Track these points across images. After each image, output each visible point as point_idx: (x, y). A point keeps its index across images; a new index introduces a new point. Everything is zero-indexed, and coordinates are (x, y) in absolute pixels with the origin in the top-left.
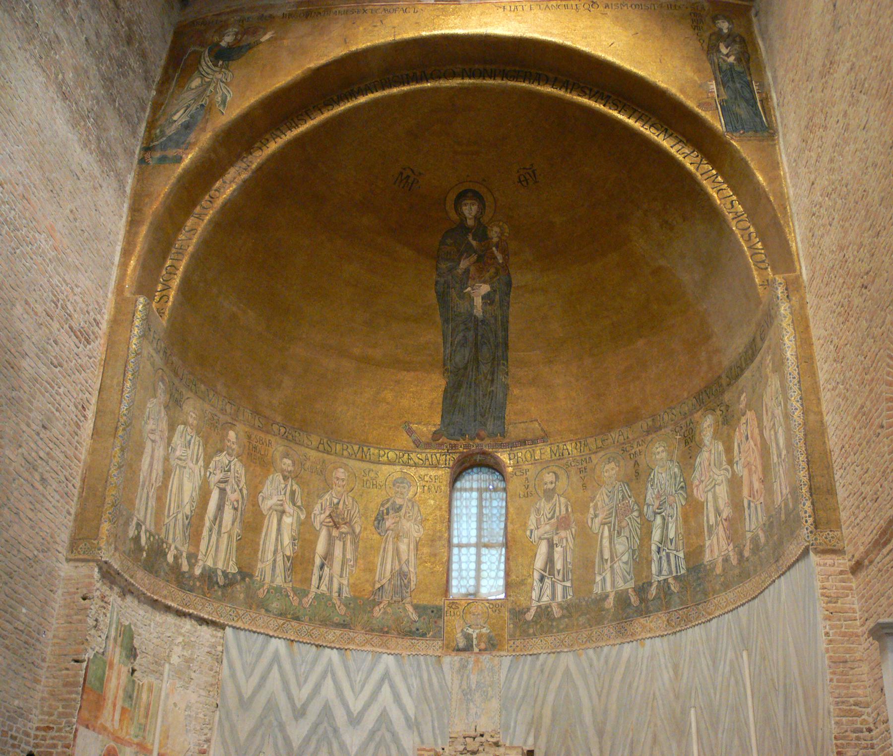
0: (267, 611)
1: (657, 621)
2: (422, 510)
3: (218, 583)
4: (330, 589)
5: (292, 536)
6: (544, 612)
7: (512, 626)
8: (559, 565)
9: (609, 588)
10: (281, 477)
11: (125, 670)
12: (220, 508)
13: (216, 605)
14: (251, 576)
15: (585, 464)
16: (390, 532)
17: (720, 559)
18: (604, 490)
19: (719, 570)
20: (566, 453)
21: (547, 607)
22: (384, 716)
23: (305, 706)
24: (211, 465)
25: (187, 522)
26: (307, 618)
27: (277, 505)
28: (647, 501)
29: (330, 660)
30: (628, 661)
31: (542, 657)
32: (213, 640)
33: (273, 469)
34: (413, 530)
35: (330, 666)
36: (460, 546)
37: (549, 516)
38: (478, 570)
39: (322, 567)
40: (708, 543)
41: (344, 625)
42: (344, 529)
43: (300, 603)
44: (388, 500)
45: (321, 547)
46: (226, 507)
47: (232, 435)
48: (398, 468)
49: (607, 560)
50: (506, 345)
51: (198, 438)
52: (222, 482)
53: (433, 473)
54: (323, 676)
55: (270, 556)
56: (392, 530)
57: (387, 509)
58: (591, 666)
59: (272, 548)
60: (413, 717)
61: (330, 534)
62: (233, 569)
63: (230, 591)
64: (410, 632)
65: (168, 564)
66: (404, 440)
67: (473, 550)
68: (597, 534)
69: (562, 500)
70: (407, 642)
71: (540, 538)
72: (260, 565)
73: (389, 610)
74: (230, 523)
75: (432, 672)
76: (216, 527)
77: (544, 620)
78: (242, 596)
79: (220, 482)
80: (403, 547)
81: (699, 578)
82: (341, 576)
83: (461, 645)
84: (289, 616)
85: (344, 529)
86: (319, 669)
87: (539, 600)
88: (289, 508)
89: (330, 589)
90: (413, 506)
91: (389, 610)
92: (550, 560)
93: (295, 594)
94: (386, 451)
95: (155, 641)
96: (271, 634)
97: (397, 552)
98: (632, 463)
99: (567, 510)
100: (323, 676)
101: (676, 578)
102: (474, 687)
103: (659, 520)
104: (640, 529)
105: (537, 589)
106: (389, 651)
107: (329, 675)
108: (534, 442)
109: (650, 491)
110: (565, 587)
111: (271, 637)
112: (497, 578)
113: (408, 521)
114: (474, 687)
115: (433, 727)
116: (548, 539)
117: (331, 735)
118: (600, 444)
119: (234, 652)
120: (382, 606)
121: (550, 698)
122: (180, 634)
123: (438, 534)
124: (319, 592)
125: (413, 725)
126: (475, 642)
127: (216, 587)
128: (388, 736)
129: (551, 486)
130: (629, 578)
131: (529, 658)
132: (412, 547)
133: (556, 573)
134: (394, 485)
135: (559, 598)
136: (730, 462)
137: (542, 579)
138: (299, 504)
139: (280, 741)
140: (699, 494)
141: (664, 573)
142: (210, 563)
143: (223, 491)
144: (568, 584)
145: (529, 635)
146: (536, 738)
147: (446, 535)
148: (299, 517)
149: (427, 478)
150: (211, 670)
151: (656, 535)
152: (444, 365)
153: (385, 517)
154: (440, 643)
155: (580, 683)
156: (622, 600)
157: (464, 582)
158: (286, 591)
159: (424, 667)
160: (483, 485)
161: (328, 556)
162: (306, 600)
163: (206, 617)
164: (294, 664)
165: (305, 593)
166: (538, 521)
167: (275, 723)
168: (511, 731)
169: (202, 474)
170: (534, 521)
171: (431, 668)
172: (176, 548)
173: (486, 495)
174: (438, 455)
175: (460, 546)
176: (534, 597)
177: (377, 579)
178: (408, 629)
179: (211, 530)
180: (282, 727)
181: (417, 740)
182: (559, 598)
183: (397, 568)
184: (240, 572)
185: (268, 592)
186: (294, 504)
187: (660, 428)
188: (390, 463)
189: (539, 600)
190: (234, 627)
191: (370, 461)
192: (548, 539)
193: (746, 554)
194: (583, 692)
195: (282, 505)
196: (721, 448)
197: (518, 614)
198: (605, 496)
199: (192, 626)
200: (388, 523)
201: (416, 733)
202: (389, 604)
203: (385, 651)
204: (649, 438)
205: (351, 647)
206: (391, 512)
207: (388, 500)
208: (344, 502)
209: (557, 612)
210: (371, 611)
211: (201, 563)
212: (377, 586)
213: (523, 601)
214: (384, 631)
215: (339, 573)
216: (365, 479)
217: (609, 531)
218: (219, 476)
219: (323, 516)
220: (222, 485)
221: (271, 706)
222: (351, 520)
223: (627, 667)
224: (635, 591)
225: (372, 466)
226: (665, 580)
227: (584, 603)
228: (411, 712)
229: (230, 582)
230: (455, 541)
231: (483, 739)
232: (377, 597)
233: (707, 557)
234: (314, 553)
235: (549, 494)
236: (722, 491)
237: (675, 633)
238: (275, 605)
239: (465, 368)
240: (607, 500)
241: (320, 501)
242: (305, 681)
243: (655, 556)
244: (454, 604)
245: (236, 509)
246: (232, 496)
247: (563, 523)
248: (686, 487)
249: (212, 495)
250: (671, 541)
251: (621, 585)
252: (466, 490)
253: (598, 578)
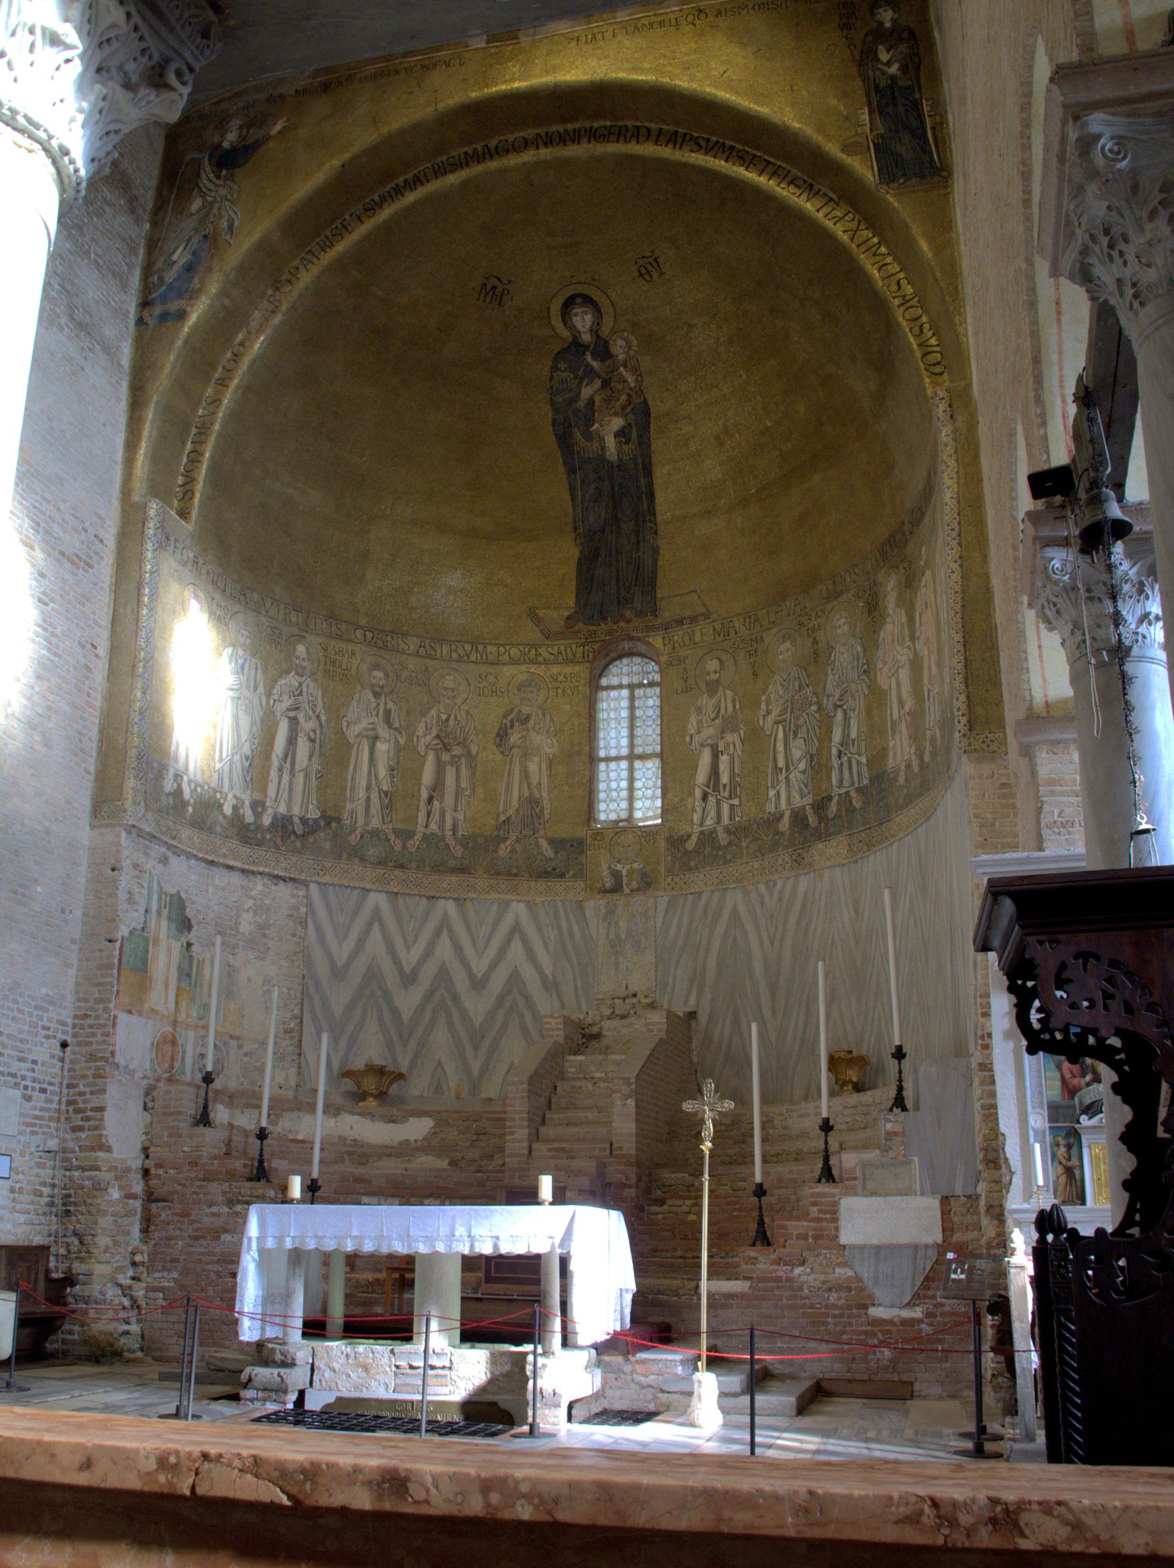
0: (362, 859)
1: (836, 847)
2: (555, 719)
3: (294, 832)
4: (442, 826)
5: (390, 766)
6: (708, 838)
7: (669, 858)
8: (725, 779)
9: (783, 805)
10: (371, 695)
11: (177, 946)
12: (292, 742)
13: (294, 859)
14: (338, 820)
15: (755, 646)
16: (515, 750)
17: (903, 766)
18: (777, 678)
19: (901, 780)
20: (732, 632)
21: (711, 832)
22: (515, 977)
23: (415, 971)
24: (275, 691)
25: (247, 764)
26: (414, 865)
27: (368, 730)
28: (828, 691)
29: (446, 914)
30: (805, 898)
31: (705, 896)
32: (294, 901)
33: (359, 686)
34: (545, 744)
35: (445, 919)
36: (608, 759)
37: (712, 716)
38: (631, 789)
39: (430, 800)
40: (891, 744)
41: (462, 870)
42: (457, 751)
43: (404, 847)
44: (512, 710)
45: (428, 776)
46: (300, 740)
47: (301, 649)
48: (523, 668)
49: (781, 769)
50: (651, 496)
51: (254, 660)
52: (292, 710)
53: (567, 670)
54: (437, 934)
55: (362, 793)
56: (519, 747)
57: (512, 721)
58: (762, 904)
59: (364, 783)
60: (551, 978)
61: (438, 759)
62: (314, 813)
63: (311, 840)
64: (545, 872)
65: (225, 817)
66: (531, 633)
67: (624, 764)
68: (770, 736)
69: (729, 693)
70: (541, 885)
71: (702, 745)
72: (349, 806)
73: (518, 848)
74: (306, 759)
75: (573, 921)
76: (288, 765)
77: (708, 850)
78: (328, 845)
79: (289, 710)
80: (533, 768)
81: (882, 790)
82: (455, 810)
83: (608, 885)
84: (391, 864)
85: (457, 751)
86: (431, 925)
87: (701, 825)
88: (383, 732)
89: (442, 826)
90: (544, 714)
91: (518, 848)
92: (715, 772)
93: (397, 836)
94: (508, 648)
95: (216, 908)
96: (368, 886)
97: (525, 774)
98: (810, 640)
99: (734, 706)
100: (437, 934)
101: (858, 790)
102: (623, 936)
103: (840, 715)
104: (819, 727)
105: (699, 810)
106: (519, 898)
107: (445, 931)
108: (693, 619)
109: (830, 677)
110: (732, 806)
111: (369, 891)
112: (653, 798)
113: (538, 733)
114: (623, 936)
115: (576, 987)
116: (712, 746)
117: (450, 1003)
118: (773, 617)
119: (321, 912)
120: (508, 843)
121: (716, 944)
122: (251, 897)
123: (576, 748)
124: (428, 831)
125: (550, 985)
126: (625, 880)
127: (293, 838)
128: (520, 1001)
129: (714, 677)
130: (806, 791)
131: (690, 897)
132: (544, 766)
133: (721, 788)
134: (519, 690)
135: (726, 820)
136: (913, 638)
137: (705, 797)
138: (397, 725)
139: (387, 1015)
140: (882, 680)
141: (846, 783)
142: (282, 809)
143: (294, 721)
144: (736, 802)
145: (689, 869)
146: (699, 998)
147: (587, 748)
148: (397, 741)
149: (561, 678)
150: (294, 935)
151: (837, 736)
152: (575, 529)
153: (510, 731)
154: (582, 885)
155: (750, 927)
156: (799, 818)
157: (613, 806)
158: (386, 834)
159: (562, 914)
160: (636, 680)
161: (438, 785)
162: (410, 843)
163: (282, 874)
164: (399, 921)
165: (410, 835)
166: (699, 722)
167: (379, 993)
168: (669, 989)
169: (264, 702)
170: (695, 724)
171: (571, 916)
172: (235, 797)
173: (639, 692)
174: (574, 647)
175: (608, 759)
176: (695, 821)
177: (501, 809)
178: (541, 869)
179: (280, 770)
180: (387, 996)
181: (557, 1004)
182: (726, 820)
183: (526, 794)
184: (324, 816)
185: (362, 837)
186: (390, 726)
187: (841, 594)
188: (514, 662)
189: (701, 825)
190: (319, 883)
191: (487, 663)
192: (712, 746)
193: (927, 758)
194: (753, 937)
195: (374, 729)
196: (904, 619)
197: (677, 842)
198: (780, 687)
199: (265, 886)
200: (514, 739)
201: (554, 995)
202: (518, 840)
203: (514, 898)
204: (829, 606)
205: (472, 895)
206: (517, 724)
207: (512, 710)
208: (456, 718)
209: (723, 838)
210: (496, 851)
211: (270, 811)
212: (503, 818)
213: (684, 828)
214: (511, 874)
215: (452, 807)
216: (482, 685)
217: (784, 731)
218: (287, 702)
219: (428, 738)
220: (292, 714)
221: (373, 974)
222: (465, 739)
223: (803, 907)
224: (813, 808)
225: (491, 669)
226: (847, 793)
227: (755, 826)
228: (548, 971)
229: (311, 828)
230: (602, 754)
231: (634, 1000)
232: (502, 832)
233: (891, 763)
234: (419, 785)
235: (713, 688)
236: (904, 674)
237: (856, 861)
238: (372, 852)
239: (603, 531)
240: (781, 691)
241: (424, 719)
242: (414, 942)
243: (835, 762)
244: (598, 834)
245: (313, 741)
246: (307, 726)
247: (730, 725)
248: (868, 671)
249: (280, 727)
250: (853, 741)
251: (798, 801)
252: (613, 688)
253: (772, 793)
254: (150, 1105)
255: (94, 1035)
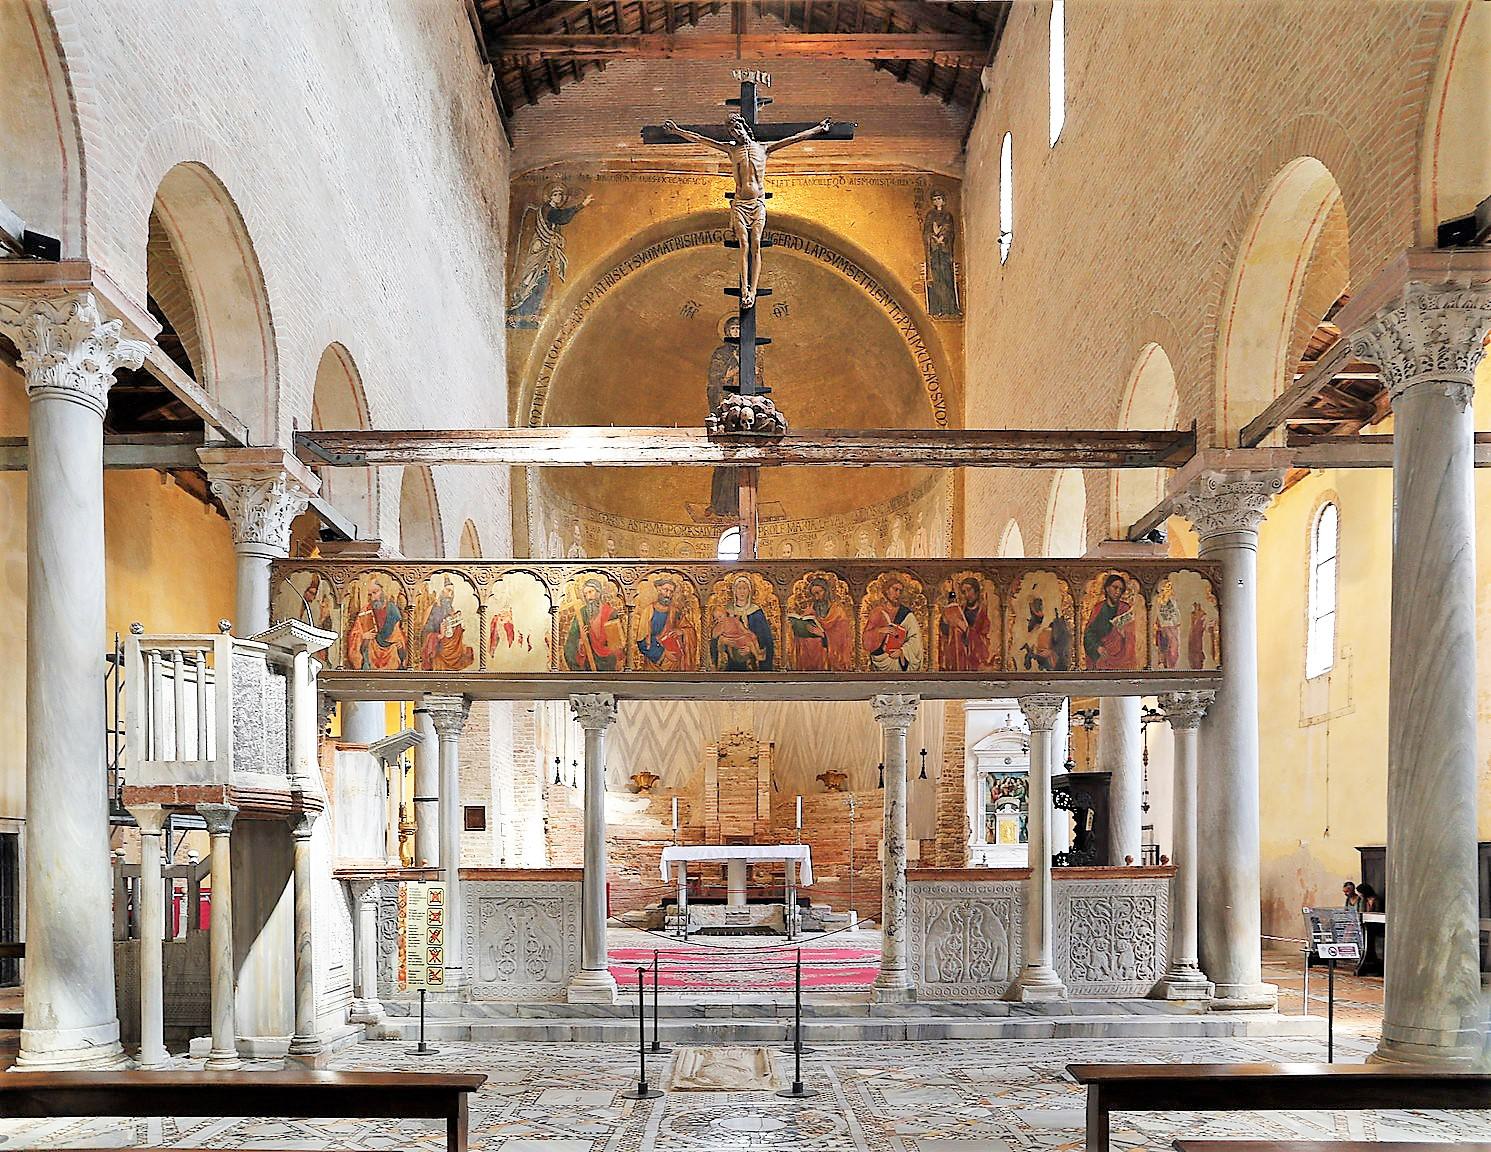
48: (682, 539)
125: (698, 726)
149: (702, 547)
225: (665, 539)
254: (546, 796)
255: (526, 761)
